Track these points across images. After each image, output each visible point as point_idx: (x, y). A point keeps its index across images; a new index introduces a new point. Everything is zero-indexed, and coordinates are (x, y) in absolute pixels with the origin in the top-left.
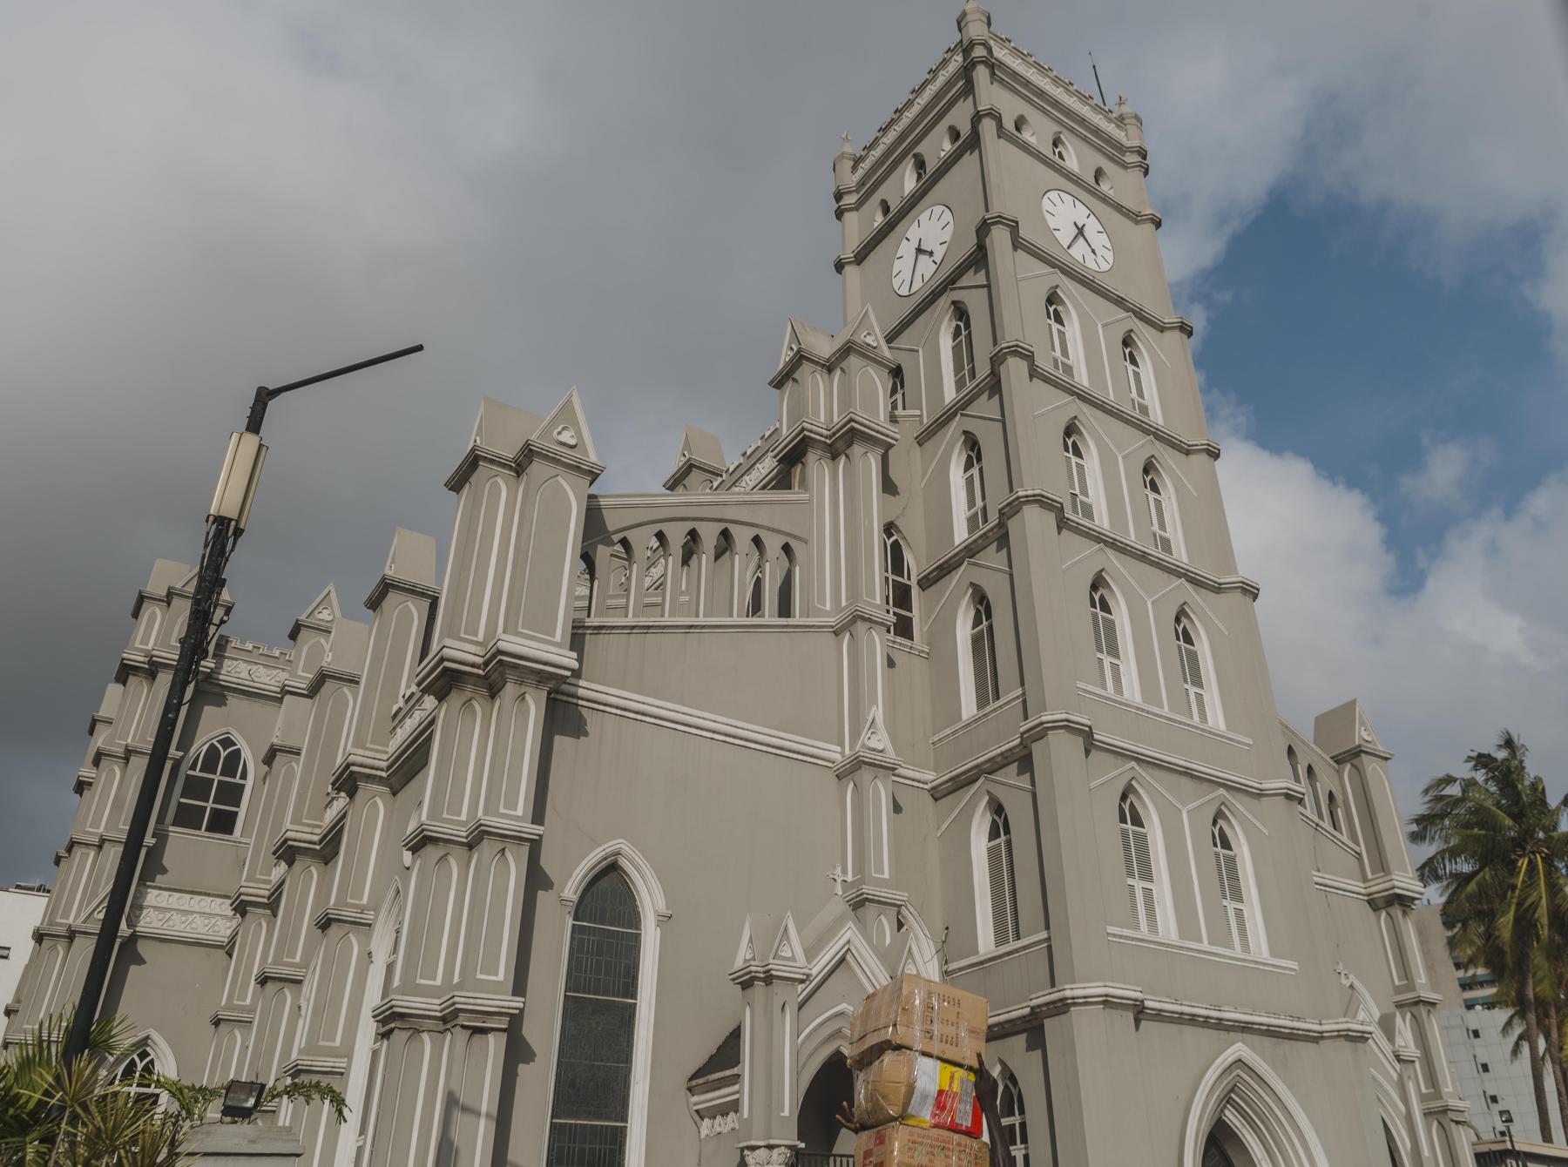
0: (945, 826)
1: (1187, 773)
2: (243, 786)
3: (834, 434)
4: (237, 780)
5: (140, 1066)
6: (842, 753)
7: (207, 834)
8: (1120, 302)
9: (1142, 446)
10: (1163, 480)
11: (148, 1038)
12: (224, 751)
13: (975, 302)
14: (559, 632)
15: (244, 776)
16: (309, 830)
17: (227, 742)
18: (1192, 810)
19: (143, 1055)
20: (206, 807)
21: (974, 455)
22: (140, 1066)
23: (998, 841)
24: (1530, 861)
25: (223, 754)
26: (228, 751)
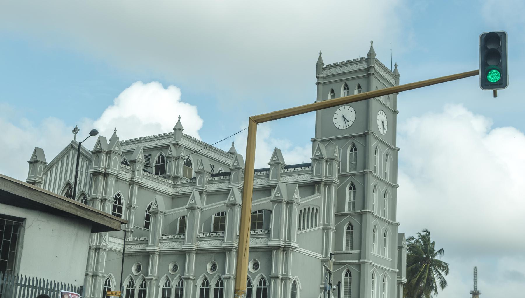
0: (336, 271)
1: (382, 268)
3: (327, 181)
5: (108, 281)
6: (323, 256)
8: (388, 145)
9: (385, 187)
10: (387, 195)
12: (118, 197)
13: (359, 147)
14: (296, 240)
15: (122, 205)
16: (195, 246)
17: (118, 195)
18: (381, 275)
20: (117, 214)
21: (352, 187)
22: (108, 281)
23: (347, 277)
24: (426, 265)
25: (118, 198)
26: (119, 197)
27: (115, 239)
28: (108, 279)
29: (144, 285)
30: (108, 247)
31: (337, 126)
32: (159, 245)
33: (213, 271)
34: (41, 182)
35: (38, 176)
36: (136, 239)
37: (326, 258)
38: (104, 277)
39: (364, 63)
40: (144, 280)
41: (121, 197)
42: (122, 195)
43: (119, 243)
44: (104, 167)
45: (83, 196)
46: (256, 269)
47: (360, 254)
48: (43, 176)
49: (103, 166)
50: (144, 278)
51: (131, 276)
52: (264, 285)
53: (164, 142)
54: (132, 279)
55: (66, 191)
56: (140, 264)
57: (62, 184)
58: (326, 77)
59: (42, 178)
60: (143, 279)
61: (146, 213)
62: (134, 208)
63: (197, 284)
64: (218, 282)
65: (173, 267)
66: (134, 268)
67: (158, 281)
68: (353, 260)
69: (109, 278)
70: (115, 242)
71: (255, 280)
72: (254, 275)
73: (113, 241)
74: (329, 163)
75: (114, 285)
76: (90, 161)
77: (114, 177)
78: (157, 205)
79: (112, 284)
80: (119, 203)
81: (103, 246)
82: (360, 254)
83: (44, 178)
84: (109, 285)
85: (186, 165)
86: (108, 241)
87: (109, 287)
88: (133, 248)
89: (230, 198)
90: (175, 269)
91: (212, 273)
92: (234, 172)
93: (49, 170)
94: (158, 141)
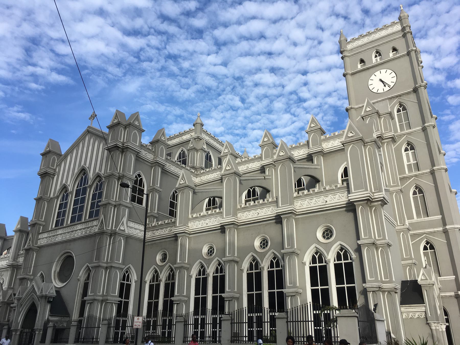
2: (144, 190)
4: (142, 188)
5: (126, 275)
7: (138, 205)
11: (129, 267)
15: (144, 187)
17: (139, 175)
19: (127, 272)
22: (126, 275)
25: (139, 179)
27: (136, 224)
28: (127, 272)
29: (171, 277)
30: (127, 232)
31: (375, 91)
32: (189, 225)
33: (263, 248)
34: (54, 173)
35: (50, 167)
36: (160, 223)
37: (403, 225)
38: (122, 269)
39: (396, 26)
40: (172, 270)
41: (142, 178)
42: (143, 177)
43: (140, 229)
44: (122, 141)
45: (98, 179)
46: (328, 238)
47: (443, 219)
48: (56, 168)
49: (121, 139)
50: (171, 268)
51: (155, 268)
52: (346, 258)
53: (185, 138)
54: (156, 271)
55: (79, 179)
56: (166, 252)
57: (76, 171)
58: (352, 50)
59: (55, 170)
60: (170, 270)
61: (170, 200)
62: (157, 191)
63: (242, 268)
64: (272, 261)
65: (208, 251)
66: (159, 257)
67: (189, 270)
68: (434, 228)
69: (129, 271)
70: (136, 227)
71: (330, 253)
72: (328, 247)
73: (133, 227)
74: (383, 118)
75: (135, 280)
76: (106, 140)
77: (134, 153)
78: (185, 179)
79: (132, 278)
80: (140, 185)
81: (120, 229)
82: (443, 219)
83: (57, 170)
84: (128, 281)
85: (207, 159)
86: (127, 226)
87: (128, 283)
88: (157, 234)
89: (279, 152)
90: (211, 252)
91: (262, 252)
92: (265, 148)
93: (62, 161)
94: (179, 138)
